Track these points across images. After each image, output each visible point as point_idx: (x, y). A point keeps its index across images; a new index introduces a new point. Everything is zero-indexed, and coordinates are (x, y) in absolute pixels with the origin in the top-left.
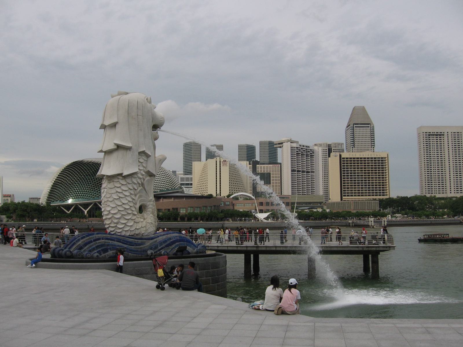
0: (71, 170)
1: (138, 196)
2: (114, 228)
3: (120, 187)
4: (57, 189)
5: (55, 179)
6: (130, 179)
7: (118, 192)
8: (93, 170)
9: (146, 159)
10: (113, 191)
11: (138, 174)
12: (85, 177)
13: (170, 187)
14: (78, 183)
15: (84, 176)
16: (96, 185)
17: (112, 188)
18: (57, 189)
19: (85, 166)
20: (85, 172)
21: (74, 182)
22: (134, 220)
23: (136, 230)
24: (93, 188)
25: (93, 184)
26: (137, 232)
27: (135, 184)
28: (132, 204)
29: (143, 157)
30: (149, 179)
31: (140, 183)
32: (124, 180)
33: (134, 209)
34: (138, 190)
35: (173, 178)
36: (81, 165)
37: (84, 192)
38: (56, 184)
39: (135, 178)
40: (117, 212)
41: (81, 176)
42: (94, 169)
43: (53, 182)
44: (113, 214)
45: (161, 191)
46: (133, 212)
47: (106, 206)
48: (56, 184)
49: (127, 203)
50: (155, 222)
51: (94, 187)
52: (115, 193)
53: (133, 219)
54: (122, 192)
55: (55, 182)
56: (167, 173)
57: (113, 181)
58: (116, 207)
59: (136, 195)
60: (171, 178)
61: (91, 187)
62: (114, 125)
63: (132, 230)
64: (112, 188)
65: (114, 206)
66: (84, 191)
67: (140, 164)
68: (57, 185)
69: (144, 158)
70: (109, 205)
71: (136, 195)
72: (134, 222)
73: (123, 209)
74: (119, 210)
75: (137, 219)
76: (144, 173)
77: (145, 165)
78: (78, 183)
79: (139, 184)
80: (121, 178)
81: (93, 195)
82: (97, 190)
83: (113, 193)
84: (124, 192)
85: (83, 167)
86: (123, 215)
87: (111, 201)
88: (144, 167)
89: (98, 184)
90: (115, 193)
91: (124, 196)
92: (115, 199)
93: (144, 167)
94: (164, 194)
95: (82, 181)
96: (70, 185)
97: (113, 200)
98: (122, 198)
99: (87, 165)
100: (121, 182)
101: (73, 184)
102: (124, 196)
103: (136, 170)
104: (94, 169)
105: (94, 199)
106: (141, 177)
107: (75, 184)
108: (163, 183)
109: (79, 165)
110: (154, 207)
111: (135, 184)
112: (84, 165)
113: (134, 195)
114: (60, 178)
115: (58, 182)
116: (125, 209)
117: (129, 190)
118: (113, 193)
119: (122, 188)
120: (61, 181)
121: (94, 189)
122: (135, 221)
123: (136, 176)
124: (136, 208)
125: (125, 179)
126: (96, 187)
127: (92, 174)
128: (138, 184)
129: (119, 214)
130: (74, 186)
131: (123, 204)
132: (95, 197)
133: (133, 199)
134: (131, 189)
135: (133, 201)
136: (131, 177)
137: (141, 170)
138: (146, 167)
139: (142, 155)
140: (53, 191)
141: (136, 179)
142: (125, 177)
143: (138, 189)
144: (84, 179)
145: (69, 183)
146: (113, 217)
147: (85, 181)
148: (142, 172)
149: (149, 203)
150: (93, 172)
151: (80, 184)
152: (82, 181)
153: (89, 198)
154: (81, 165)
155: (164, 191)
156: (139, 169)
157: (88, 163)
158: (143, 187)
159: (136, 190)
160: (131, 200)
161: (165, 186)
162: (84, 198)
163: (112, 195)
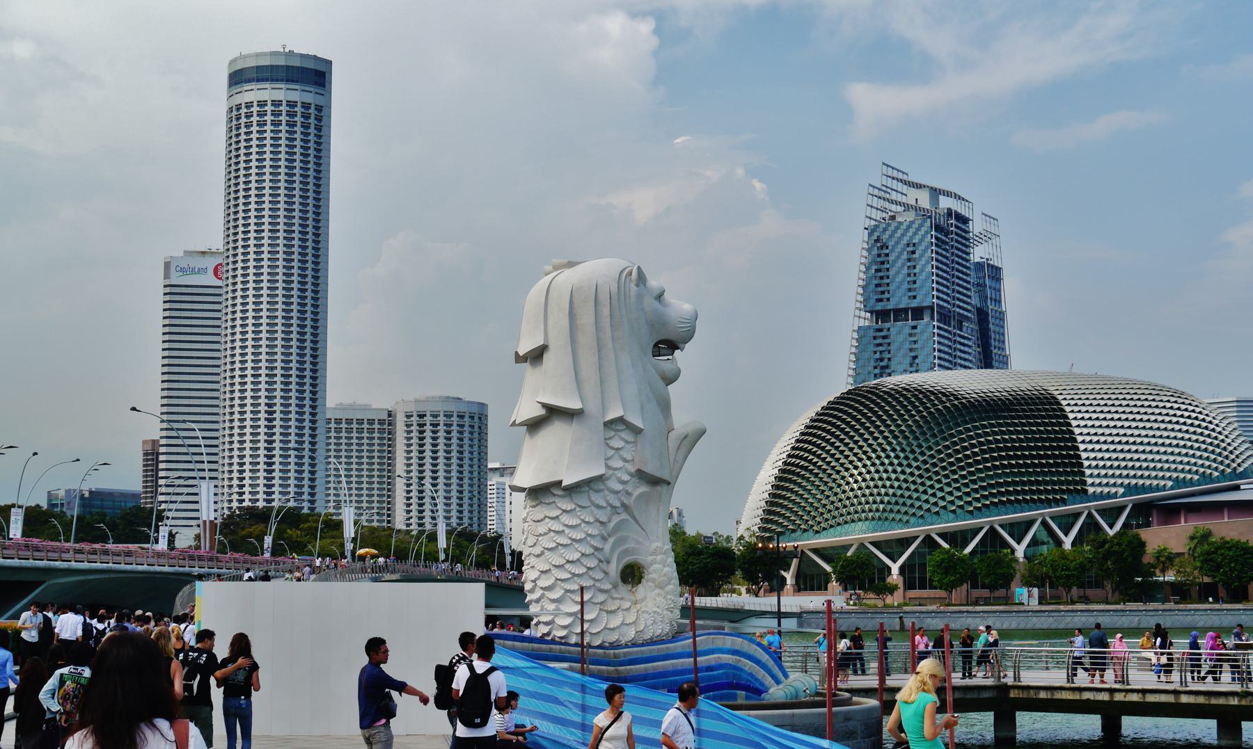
0: (854, 417)
1: (611, 540)
2: (550, 627)
3: (557, 517)
4: (799, 485)
5: (784, 456)
6: (586, 495)
7: (554, 531)
8: (917, 418)
9: (630, 438)
10: (542, 529)
11: (608, 479)
12: (890, 444)
13: (1216, 469)
14: (865, 466)
15: (885, 438)
16: (927, 470)
17: (538, 521)
18: (799, 485)
19: (889, 403)
20: (879, 426)
21: (851, 462)
22: (601, 603)
23: (607, 632)
24: (919, 481)
25: (918, 468)
26: (613, 637)
27: (599, 507)
28: (592, 563)
29: (620, 434)
30: (646, 492)
31: (618, 504)
32: (568, 499)
33: (599, 575)
34: (611, 525)
35: (1226, 433)
36: (873, 401)
37: (886, 499)
38: (789, 472)
39: (598, 491)
41: (876, 439)
42: (919, 412)
43: (780, 463)
44: (542, 588)
45: (1178, 483)
46: (598, 585)
47: (529, 567)
48: (789, 472)
49: (578, 560)
50: (672, 612)
51: (920, 476)
52: (545, 534)
53: (597, 603)
54: (563, 531)
55: (785, 463)
56: (1207, 415)
57: (541, 502)
58: (550, 569)
59: (605, 539)
60: (1220, 433)
61: (911, 479)
62: (537, 356)
63: (594, 631)
64: (538, 521)
65: (546, 567)
66: (887, 494)
67: (611, 452)
68: (793, 473)
69: (623, 436)
70: (533, 567)
71: (605, 539)
72: (600, 609)
73: (570, 576)
75: (610, 601)
76: (626, 477)
77: (629, 457)
78: (865, 466)
79: (614, 507)
80: (560, 493)
81: (920, 508)
82: (932, 487)
83: (541, 535)
84: (567, 531)
85: (882, 408)
86: (567, 591)
87: (538, 556)
88: (625, 460)
89: (935, 465)
90: (545, 534)
91: (569, 542)
92: (547, 549)
93: (625, 460)
94: (1193, 494)
95: (879, 457)
96: (838, 472)
97: (542, 553)
98: (562, 545)
99: (896, 399)
100: (559, 505)
101: (847, 470)
102: (569, 542)
103: (599, 470)
104: (919, 412)
105: (921, 521)
106: (618, 487)
107: (856, 468)
108: (1201, 457)
109: (869, 399)
110: (666, 569)
111: (599, 507)
112: (884, 400)
114: (801, 449)
115: (797, 466)
116: (574, 575)
117: (583, 525)
118: (541, 535)
119: (562, 520)
120: (805, 459)
121: (923, 484)
123: (603, 487)
124: (606, 573)
125: (570, 495)
126: (930, 478)
127: (913, 432)
128: (609, 508)
129: (558, 589)
130: (852, 476)
131: (568, 562)
132: (927, 515)
133: (596, 549)
134: (588, 523)
135: (596, 553)
136: (587, 489)
137: (616, 469)
138: (633, 460)
139: (618, 428)
140: (780, 496)
141: (601, 494)
142: (573, 490)
143: (609, 522)
144: (884, 450)
145: (833, 468)
146: (542, 596)
147: (888, 457)
148: (619, 475)
149: (652, 558)
150: (915, 422)
151: (872, 469)
152: (879, 457)
153: (905, 518)
154: (873, 401)
155: (1191, 483)
156: (608, 467)
157: (898, 392)
158: (629, 515)
159: (602, 523)
160: (589, 550)
161: (1195, 464)
162: (887, 519)
163: (540, 538)
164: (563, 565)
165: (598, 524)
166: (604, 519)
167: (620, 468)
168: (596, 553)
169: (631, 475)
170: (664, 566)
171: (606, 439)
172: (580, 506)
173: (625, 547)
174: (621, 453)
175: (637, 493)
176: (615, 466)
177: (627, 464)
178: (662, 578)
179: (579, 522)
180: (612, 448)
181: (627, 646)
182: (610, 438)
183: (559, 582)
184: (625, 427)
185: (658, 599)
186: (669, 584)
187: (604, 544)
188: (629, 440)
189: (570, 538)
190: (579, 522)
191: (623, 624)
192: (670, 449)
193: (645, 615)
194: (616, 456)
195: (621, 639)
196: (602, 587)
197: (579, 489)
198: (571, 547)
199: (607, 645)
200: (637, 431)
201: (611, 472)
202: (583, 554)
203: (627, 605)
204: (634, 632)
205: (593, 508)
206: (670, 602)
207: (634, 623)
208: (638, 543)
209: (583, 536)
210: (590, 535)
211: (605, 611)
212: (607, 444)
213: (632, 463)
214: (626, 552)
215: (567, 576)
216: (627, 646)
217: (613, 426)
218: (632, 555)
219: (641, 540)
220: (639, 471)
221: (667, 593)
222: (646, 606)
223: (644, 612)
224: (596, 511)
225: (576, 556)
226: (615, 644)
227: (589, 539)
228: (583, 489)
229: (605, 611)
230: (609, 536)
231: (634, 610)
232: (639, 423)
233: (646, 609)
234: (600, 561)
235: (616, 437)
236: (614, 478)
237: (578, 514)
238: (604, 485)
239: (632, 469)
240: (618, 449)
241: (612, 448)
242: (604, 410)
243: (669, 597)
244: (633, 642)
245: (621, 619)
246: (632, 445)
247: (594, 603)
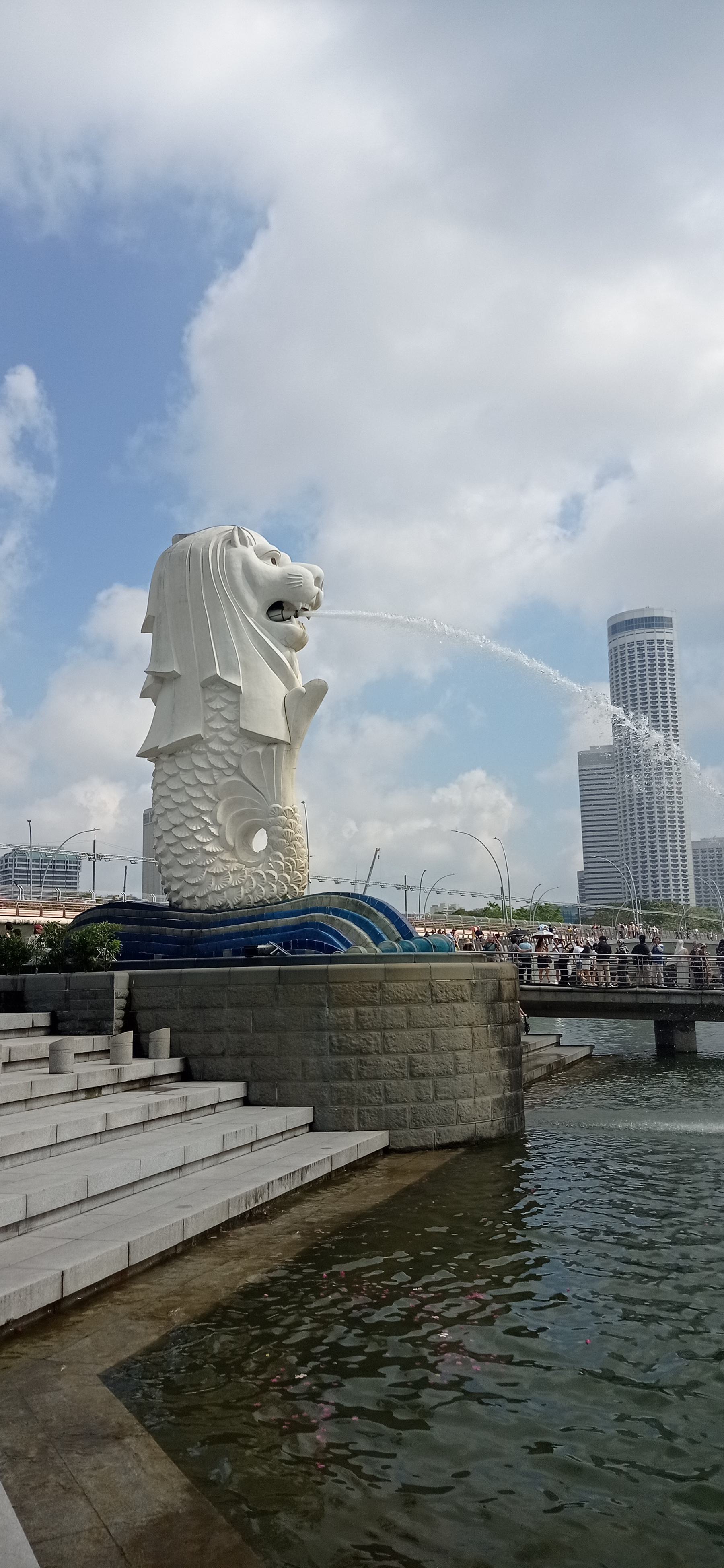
9: (233, 699)
11: (209, 741)
27: (201, 769)
29: (221, 695)
31: (224, 766)
39: (199, 753)
40: (164, 850)
74: (168, 845)
75: (220, 865)
79: (218, 769)
86: (176, 856)
111: (201, 769)
122: (209, 871)
123: (204, 749)
131: (176, 826)
133: (202, 812)
134: (189, 785)
136: (189, 752)
137: (217, 730)
139: (218, 689)
164: (170, 831)
167: (222, 730)
171: (206, 701)
174: (223, 713)
182: (210, 700)
190: (183, 785)
200: (237, 690)
201: (212, 734)
205: (196, 771)
208: (253, 804)
211: (212, 873)
214: (242, 814)
217: (213, 688)
224: (198, 774)
228: (184, 752)
232: (238, 681)
234: (208, 824)
238: (207, 747)
247: (199, 866)
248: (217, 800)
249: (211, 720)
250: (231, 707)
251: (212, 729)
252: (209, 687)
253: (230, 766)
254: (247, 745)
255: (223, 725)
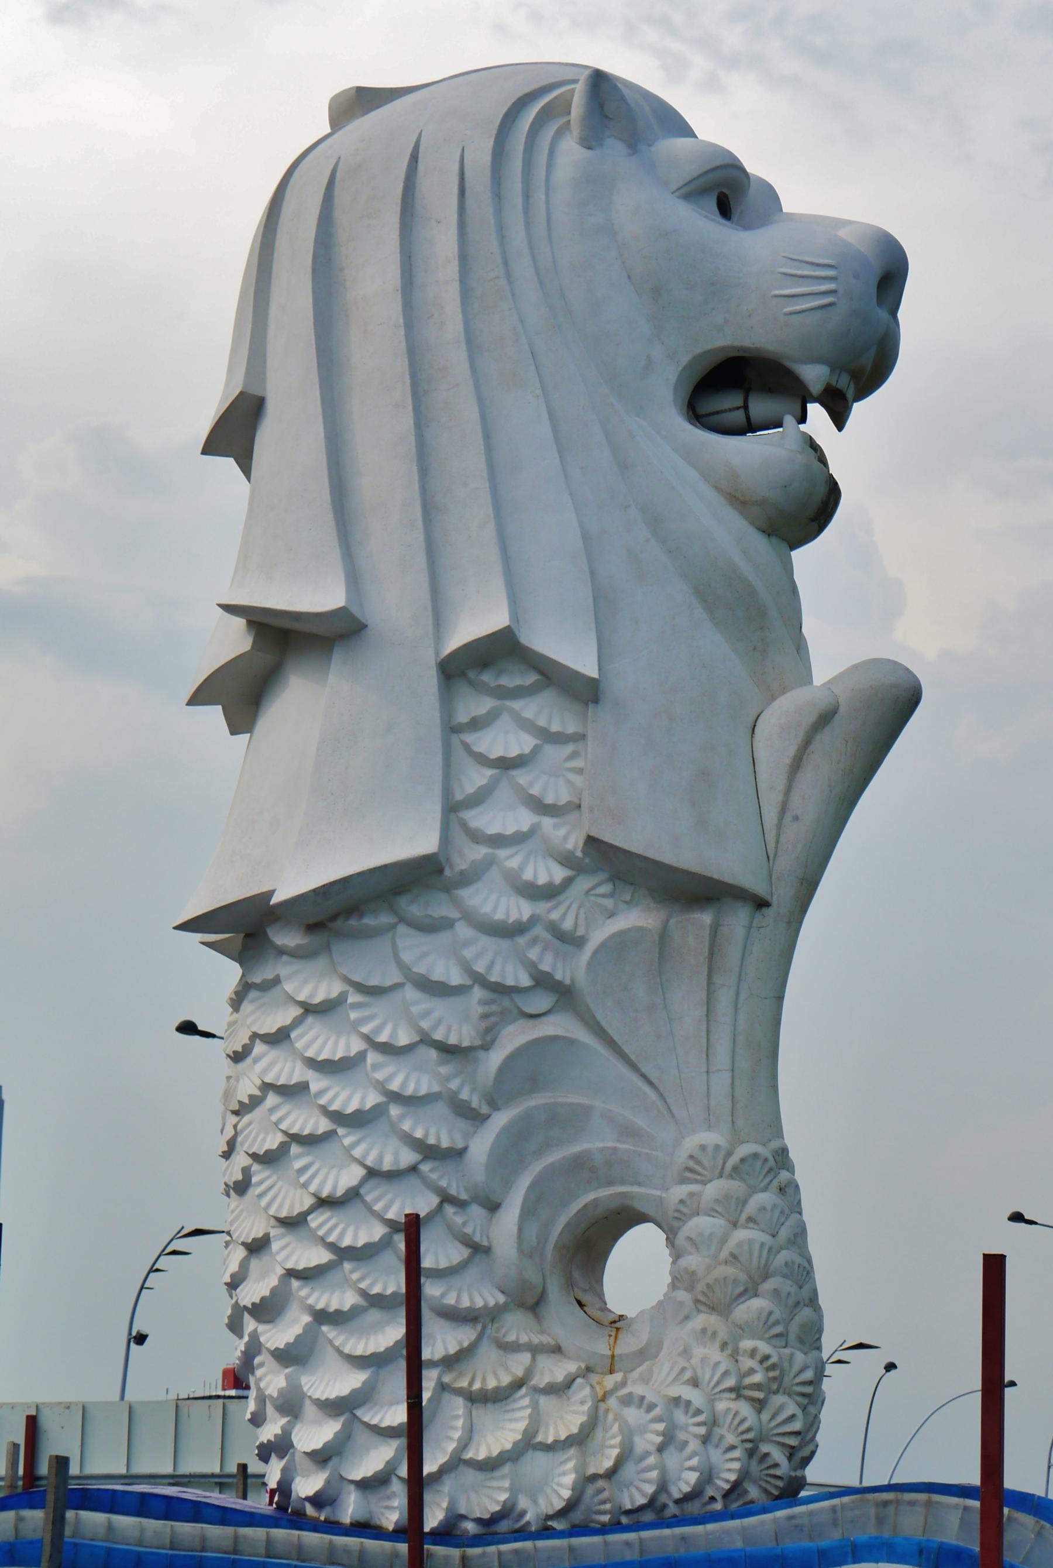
1: (500, 1120)
11: (466, 879)
23: (470, 1476)
29: (516, 705)
34: (495, 1058)
39: (430, 927)
59: (475, 1118)
67: (476, 778)
77: (558, 793)
88: (541, 807)
93: (541, 807)
113: (441, 1108)
117: (372, 1057)
128: (478, 993)
133: (429, 1152)
134: (387, 1049)
137: (498, 841)
141: (443, 938)
143: (486, 1047)
149: (679, 1192)
159: (448, 1051)
165: (433, 1053)
166: (463, 1034)
167: (518, 839)
168: (425, 1167)
169: (566, 860)
170: (735, 1225)
172: (361, 988)
173: (575, 1149)
174: (522, 777)
175: (598, 937)
176: (492, 830)
177: (547, 822)
178: (730, 1271)
179: (356, 1046)
180: (483, 760)
181: (545, 1532)
183: (295, 1284)
184: (532, 678)
185: (698, 1351)
186: (750, 1291)
187: (468, 1136)
188: (555, 727)
189: (325, 1111)
191: (528, 1444)
192: (761, 767)
193: (632, 1415)
194: (504, 793)
195: (523, 1503)
196: (465, 1303)
197: (353, 922)
198: (327, 1147)
199: (470, 1527)
201: (478, 852)
202: (372, 1173)
203: (555, 1370)
204: (569, 1479)
206: (747, 1363)
207: (572, 1441)
208: (629, 1132)
209: (372, 1099)
210: (396, 1097)
212: (467, 747)
213: (573, 816)
215: (320, 1256)
216: (545, 1532)
217: (486, 677)
218: (610, 1183)
219: (640, 1122)
220: (591, 841)
221: (743, 1329)
222: (646, 1380)
223: (627, 1401)
225: (350, 1177)
226: (504, 1526)
227: (394, 1111)
228: (368, 921)
229: (459, 1392)
230: (494, 1105)
231: (582, 1392)
233: (639, 1390)
235: (505, 720)
236: (494, 874)
237: (353, 1015)
238: (456, 903)
239: (574, 843)
240: (506, 764)
241: (483, 760)
242: (439, 625)
243: (747, 1344)
244: (577, 1516)
245: (522, 1425)
246: (570, 748)
248: (485, 1109)
249: (477, 800)
250: (554, 754)
251: (476, 837)
252: (472, 674)
253: (543, 981)
254: (609, 903)
255: (522, 819)
